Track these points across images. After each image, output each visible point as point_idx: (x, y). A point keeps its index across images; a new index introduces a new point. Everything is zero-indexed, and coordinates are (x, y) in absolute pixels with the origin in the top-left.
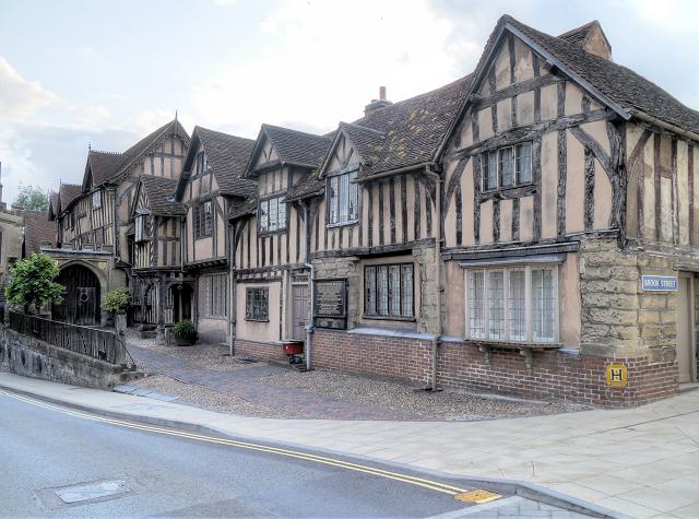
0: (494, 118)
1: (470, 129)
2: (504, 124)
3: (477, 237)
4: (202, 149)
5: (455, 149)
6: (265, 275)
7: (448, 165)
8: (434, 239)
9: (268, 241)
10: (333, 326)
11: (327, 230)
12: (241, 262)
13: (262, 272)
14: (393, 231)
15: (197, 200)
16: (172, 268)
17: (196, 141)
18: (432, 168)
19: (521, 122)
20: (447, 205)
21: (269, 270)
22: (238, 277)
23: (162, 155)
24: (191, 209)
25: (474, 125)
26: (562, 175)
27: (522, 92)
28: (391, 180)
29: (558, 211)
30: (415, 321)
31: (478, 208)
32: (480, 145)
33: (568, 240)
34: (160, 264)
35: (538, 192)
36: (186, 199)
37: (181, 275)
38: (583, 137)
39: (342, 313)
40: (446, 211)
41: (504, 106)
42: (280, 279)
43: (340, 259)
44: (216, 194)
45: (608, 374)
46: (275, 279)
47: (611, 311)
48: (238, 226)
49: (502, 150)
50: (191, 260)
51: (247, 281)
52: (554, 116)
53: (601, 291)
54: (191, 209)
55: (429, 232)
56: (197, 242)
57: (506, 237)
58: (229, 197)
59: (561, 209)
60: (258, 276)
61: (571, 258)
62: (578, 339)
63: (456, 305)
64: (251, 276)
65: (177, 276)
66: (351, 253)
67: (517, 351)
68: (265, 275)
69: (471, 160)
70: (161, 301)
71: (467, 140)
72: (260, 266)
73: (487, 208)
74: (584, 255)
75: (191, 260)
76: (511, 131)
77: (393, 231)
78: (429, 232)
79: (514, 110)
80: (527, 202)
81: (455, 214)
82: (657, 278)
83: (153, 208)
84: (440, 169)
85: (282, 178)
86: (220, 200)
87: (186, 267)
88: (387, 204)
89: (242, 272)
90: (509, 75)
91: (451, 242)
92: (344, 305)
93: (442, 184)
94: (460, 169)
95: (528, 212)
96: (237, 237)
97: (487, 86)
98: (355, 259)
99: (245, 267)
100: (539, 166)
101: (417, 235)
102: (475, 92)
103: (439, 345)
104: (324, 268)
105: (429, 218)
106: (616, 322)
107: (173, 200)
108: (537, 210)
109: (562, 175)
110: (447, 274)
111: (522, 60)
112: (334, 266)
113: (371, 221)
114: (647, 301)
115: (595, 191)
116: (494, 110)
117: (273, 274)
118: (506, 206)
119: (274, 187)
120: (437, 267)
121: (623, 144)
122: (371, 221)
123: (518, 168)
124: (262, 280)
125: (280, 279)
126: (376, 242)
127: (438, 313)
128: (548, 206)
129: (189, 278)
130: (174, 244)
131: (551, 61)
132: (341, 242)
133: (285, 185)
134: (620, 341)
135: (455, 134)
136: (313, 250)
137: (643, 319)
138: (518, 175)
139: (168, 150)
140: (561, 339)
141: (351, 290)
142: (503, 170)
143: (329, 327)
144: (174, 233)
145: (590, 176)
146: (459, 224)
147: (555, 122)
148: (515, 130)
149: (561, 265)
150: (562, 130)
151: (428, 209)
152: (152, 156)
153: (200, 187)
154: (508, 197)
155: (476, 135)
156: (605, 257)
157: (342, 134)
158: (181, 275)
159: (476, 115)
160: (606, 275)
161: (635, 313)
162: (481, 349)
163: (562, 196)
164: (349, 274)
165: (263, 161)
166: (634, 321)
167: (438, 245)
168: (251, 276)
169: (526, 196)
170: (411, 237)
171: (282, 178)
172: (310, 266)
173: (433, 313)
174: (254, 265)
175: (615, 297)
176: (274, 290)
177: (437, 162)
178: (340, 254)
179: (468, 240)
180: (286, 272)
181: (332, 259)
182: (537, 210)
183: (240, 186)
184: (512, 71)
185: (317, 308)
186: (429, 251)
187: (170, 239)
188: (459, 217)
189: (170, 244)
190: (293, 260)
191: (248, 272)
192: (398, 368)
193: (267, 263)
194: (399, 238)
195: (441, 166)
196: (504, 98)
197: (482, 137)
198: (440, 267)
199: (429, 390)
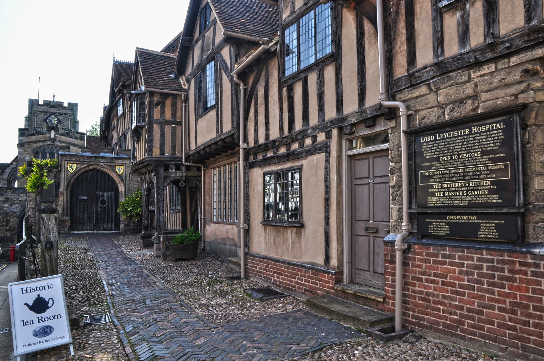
42: (325, 148)
60: (283, 150)
68: (295, 146)
96: (250, 96)
112: (469, 90)
117: (308, 141)
124: (290, 156)
180: (335, 132)
193: (298, 126)
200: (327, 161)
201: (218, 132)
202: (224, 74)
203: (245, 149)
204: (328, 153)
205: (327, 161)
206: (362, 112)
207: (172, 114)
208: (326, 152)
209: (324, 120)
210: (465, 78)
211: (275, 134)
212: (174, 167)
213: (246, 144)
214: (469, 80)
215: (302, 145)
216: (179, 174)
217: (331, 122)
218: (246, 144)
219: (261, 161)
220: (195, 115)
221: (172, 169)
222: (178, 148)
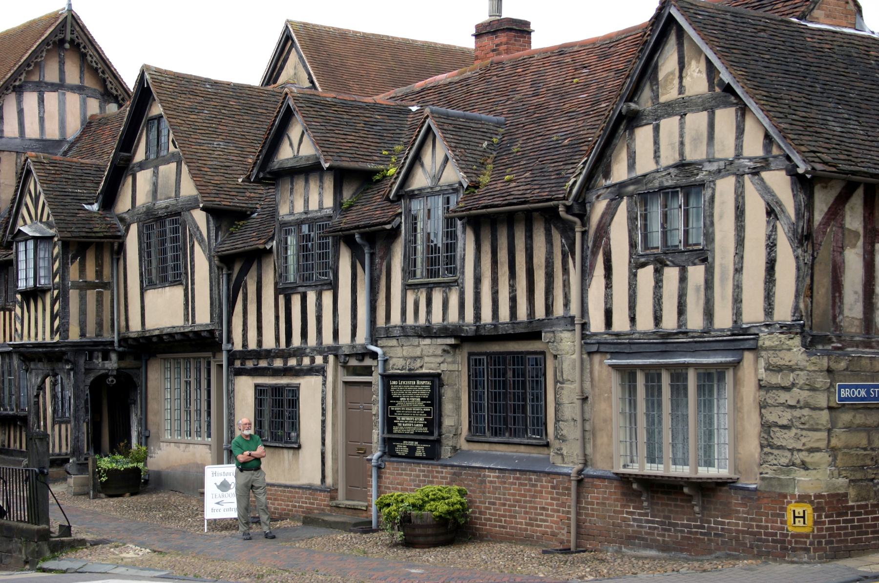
0: (656, 142)
1: (624, 155)
2: (669, 157)
3: (633, 320)
4: (156, 109)
5: (604, 183)
6: (292, 362)
7: (592, 206)
8: (572, 318)
9: (296, 300)
10: (418, 454)
12: (241, 334)
13: (285, 355)
14: (513, 300)
16: (96, 344)
17: (144, 94)
18: (568, 209)
19: (690, 157)
20: (593, 267)
21: (299, 353)
22: (238, 364)
23: (41, 87)
24: (134, 228)
25: (628, 148)
26: (740, 242)
27: (692, 111)
28: (510, 219)
29: (734, 290)
30: (547, 445)
31: (633, 276)
32: (636, 181)
33: (745, 332)
34: (74, 335)
35: (710, 260)
36: (123, 205)
37: (114, 356)
38: (765, 190)
39: (431, 433)
40: (591, 275)
41: (669, 125)
43: (428, 341)
44: (192, 204)
45: (789, 517)
46: (312, 371)
47: (794, 431)
48: (237, 269)
49: (667, 193)
50: (135, 326)
51: (256, 372)
52: (730, 154)
53: (782, 404)
54: (134, 228)
55: (566, 304)
56: (150, 295)
57: (670, 322)
58: (215, 213)
59: (738, 288)
60: (278, 363)
61: (748, 357)
62: (756, 470)
63: (605, 421)
64: (263, 364)
65: (106, 357)
66: (445, 331)
67: (682, 487)
68: (292, 362)
69: (625, 199)
70: (55, 411)
71: (620, 172)
72: (283, 345)
73: (646, 275)
74: (763, 353)
75: (135, 326)
76: (676, 166)
77: (513, 300)
78: (566, 304)
79: (682, 136)
80: (697, 273)
81: (603, 282)
82: (862, 387)
83: (60, 223)
84: (582, 212)
85: (321, 187)
86: (200, 217)
87: (123, 340)
88: (503, 256)
89: (246, 354)
90: (676, 81)
91: (597, 324)
92: (434, 422)
93: (584, 233)
94: (610, 213)
95: (698, 289)
96: (236, 289)
97: (646, 93)
98: (452, 341)
99: (252, 345)
100: (712, 224)
101: (549, 309)
102: (630, 99)
103: (580, 482)
104: (400, 356)
105: (566, 284)
106: (799, 446)
107: (95, 207)
108: (709, 284)
109: (740, 242)
110: (591, 372)
111: (693, 63)
112: (418, 352)
113: (478, 281)
114: (846, 417)
115: (778, 267)
116: (657, 129)
117: (306, 361)
118: (671, 274)
119: (306, 202)
120: (578, 364)
121: (810, 206)
122: (478, 281)
123: (686, 223)
124: (286, 371)
125: (320, 371)
126: (487, 316)
127: (578, 434)
128: (723, 280)
129: (129, 363)
130: (100, 296)
131: (726, 76)
132: (429, 312)
133: (329, 202)
134: (803, 472)
135: (601, 164)
136: (381, 322)
137: (834, 442)
138: (686, 233)
139: (51, 74)
140: (736, 469)
141: (448, 393)
142: (670, 223)
143: (411, 455)
144: (99, 273)
145: (771, 246)
146: (608, 297)
147: (731, 163)
148: (682, 166)
149: (736, 365)
150: (740, 176)
151: (566, 271)
152: (19, 90)
153: (155, 185)
154: (675, 265)
155: (631, 166)
156: (787, 359)
157: (429, 128)
158: (114, 356)
159: (632, 133)
160: (786, 383)
161: (824, 435)
162: (635, 486)
163: (738, 270)
164: (444, 367)
165: (286, 154)
166: (823, 445)
167: (578, 328)
168: (263, 364)
169: (695, 264)
170: (540, 312)
171: (321, 187)
172: (379, 350)
173: (572, 432)
174: (269, 343)
175: (797, 413)
176: (310, 389)
177: (576, 199)
178: (427, 332)
179: (620, 323)
180: (331, 358)
181: (415, 341)
182: (709, 284)
183: (238, 191)
184: (681, 78)
185: (390, 423)
186: (566, 335)
187: (92, 286)
188: (609, 286)
189: (91, 295)
190: (345, 338)
191: (260, 354)
192: (521, 520)
193: (296, 341)
194: (522, 314)
195: (583, 205)
196: (670, 115)
197: (640, 170)
198: (582, 361)
199: (567, 551)
200: (324, 384)
201: (186, 319)
202: (196, 244)
203: (229, 351)
204: (325, 377)
205: (324, 384)
206: (354, 347)
207: (97, 271)
208: (323, 375)
209: (321, 343)
210: (417, 343)
212: (100, 355)
213: (230, 346)
214: (419, 346)
215: (299, 363)
217: (329, 347)
218: (230, 346)
219: (252, 369)
220: (142, 282)
221: (97, 358)
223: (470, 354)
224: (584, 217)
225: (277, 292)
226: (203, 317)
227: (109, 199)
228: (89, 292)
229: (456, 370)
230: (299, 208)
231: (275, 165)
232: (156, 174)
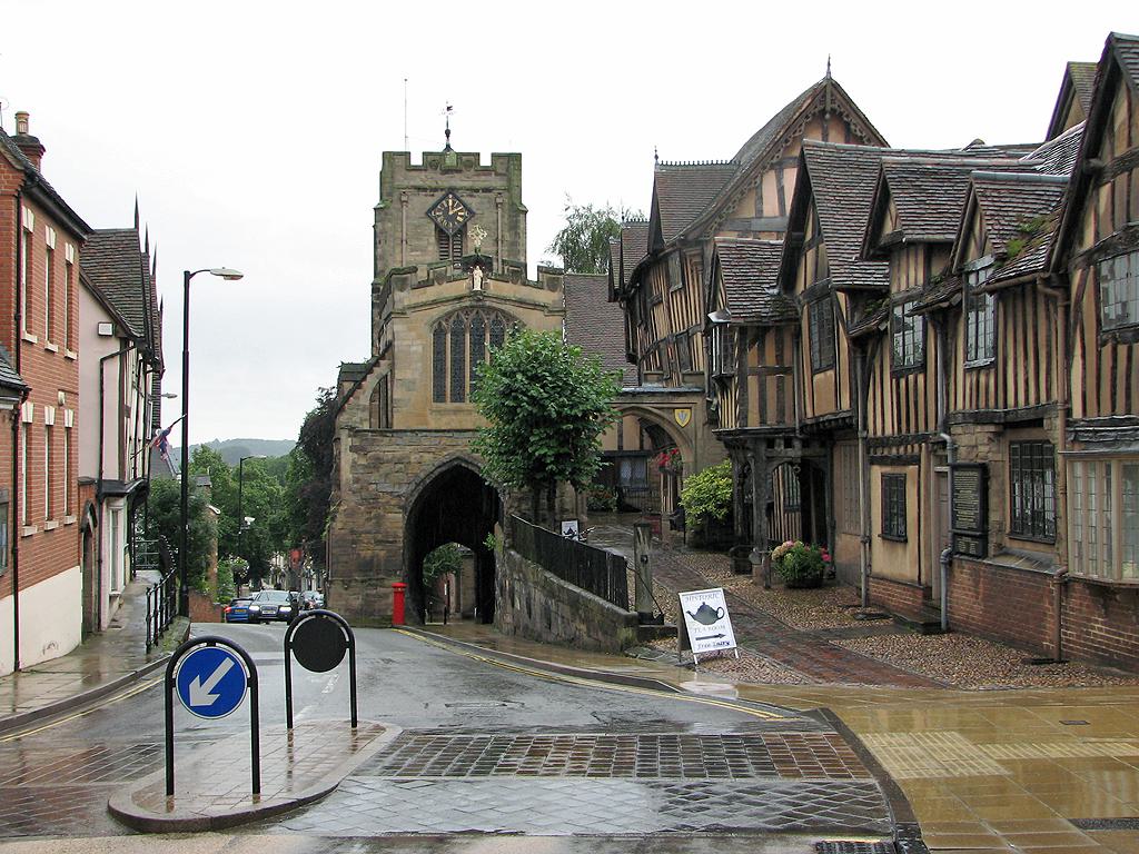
9: (903, 382)
11: (966, 371)
15: (812, 289)
31: (1099, 354)
37: (797, 444)
51: (882, 461)
86: (841, 296)
93: (1067, 308)
96: (868, 372)
98: (992, 428)
125: (916, 460)
141: (994, 486)
158: (797, 444)
171: (916, 262)
181: (971, 426)
185: (955, 518)
191: (884, 442)
211: (888, 432)
216: (790, 452)
222: (788, 412)
223: (1011, 443)
224: (1067, 289)
225: (893, 374)
226: (845, 403)
227: (788, 278)
228: (769, 378)
229: (996, 455)
230: (903, 287)
231: (882, 242)
232: (817, 252)
